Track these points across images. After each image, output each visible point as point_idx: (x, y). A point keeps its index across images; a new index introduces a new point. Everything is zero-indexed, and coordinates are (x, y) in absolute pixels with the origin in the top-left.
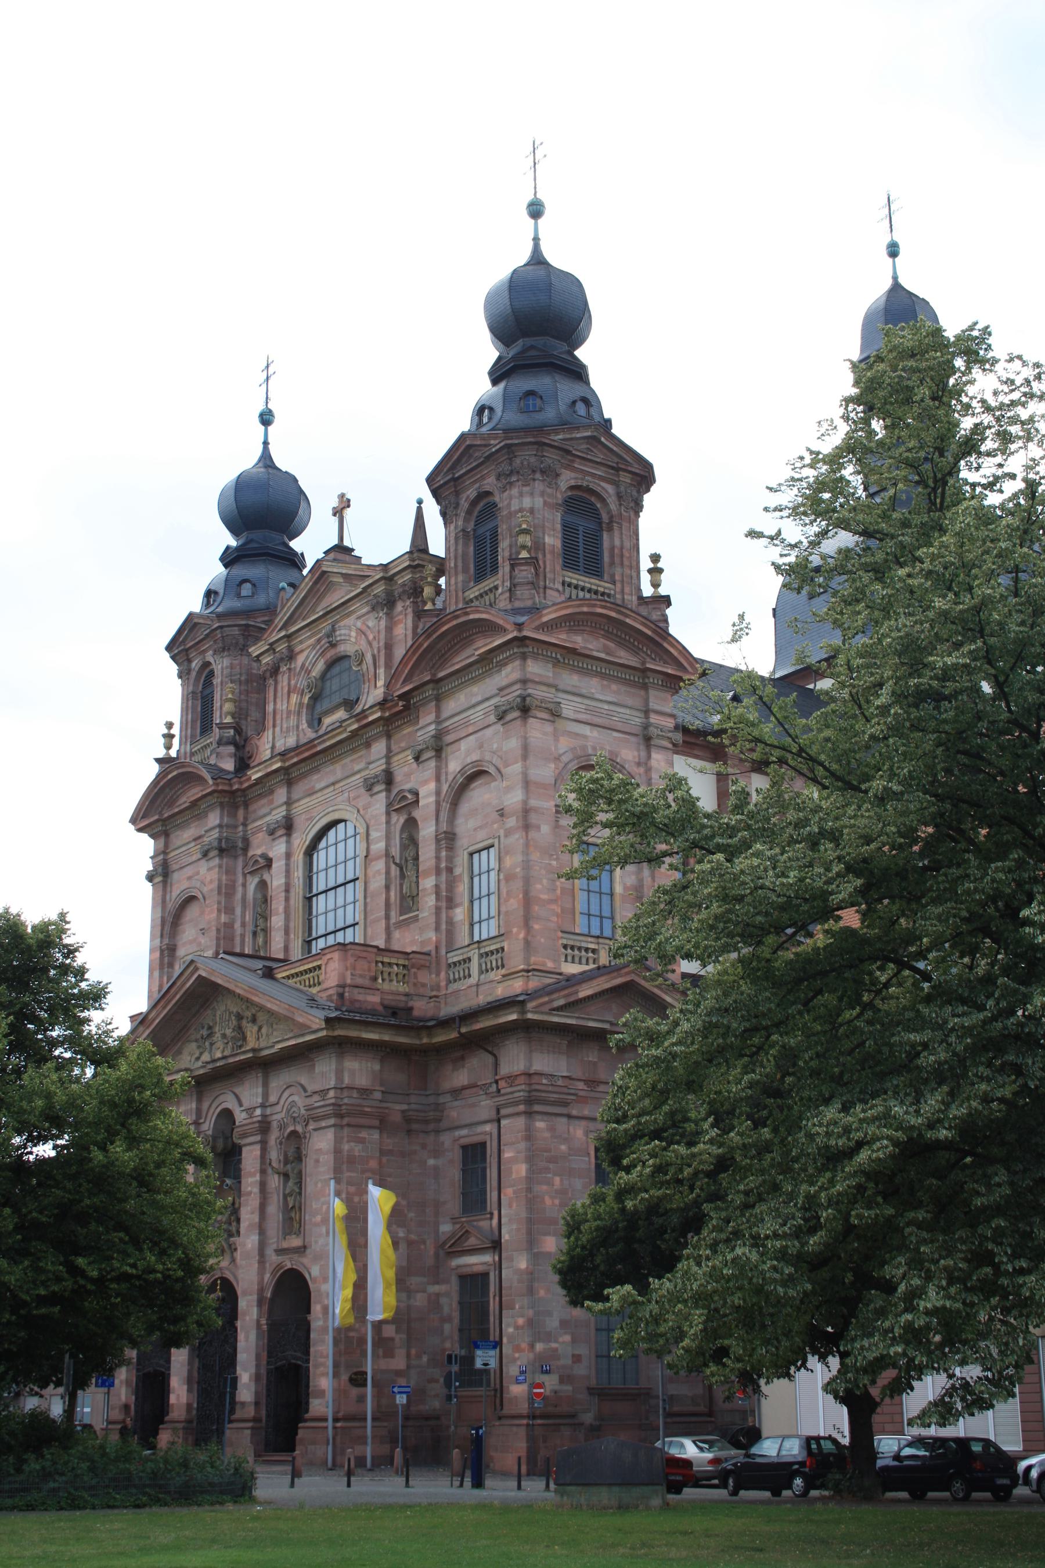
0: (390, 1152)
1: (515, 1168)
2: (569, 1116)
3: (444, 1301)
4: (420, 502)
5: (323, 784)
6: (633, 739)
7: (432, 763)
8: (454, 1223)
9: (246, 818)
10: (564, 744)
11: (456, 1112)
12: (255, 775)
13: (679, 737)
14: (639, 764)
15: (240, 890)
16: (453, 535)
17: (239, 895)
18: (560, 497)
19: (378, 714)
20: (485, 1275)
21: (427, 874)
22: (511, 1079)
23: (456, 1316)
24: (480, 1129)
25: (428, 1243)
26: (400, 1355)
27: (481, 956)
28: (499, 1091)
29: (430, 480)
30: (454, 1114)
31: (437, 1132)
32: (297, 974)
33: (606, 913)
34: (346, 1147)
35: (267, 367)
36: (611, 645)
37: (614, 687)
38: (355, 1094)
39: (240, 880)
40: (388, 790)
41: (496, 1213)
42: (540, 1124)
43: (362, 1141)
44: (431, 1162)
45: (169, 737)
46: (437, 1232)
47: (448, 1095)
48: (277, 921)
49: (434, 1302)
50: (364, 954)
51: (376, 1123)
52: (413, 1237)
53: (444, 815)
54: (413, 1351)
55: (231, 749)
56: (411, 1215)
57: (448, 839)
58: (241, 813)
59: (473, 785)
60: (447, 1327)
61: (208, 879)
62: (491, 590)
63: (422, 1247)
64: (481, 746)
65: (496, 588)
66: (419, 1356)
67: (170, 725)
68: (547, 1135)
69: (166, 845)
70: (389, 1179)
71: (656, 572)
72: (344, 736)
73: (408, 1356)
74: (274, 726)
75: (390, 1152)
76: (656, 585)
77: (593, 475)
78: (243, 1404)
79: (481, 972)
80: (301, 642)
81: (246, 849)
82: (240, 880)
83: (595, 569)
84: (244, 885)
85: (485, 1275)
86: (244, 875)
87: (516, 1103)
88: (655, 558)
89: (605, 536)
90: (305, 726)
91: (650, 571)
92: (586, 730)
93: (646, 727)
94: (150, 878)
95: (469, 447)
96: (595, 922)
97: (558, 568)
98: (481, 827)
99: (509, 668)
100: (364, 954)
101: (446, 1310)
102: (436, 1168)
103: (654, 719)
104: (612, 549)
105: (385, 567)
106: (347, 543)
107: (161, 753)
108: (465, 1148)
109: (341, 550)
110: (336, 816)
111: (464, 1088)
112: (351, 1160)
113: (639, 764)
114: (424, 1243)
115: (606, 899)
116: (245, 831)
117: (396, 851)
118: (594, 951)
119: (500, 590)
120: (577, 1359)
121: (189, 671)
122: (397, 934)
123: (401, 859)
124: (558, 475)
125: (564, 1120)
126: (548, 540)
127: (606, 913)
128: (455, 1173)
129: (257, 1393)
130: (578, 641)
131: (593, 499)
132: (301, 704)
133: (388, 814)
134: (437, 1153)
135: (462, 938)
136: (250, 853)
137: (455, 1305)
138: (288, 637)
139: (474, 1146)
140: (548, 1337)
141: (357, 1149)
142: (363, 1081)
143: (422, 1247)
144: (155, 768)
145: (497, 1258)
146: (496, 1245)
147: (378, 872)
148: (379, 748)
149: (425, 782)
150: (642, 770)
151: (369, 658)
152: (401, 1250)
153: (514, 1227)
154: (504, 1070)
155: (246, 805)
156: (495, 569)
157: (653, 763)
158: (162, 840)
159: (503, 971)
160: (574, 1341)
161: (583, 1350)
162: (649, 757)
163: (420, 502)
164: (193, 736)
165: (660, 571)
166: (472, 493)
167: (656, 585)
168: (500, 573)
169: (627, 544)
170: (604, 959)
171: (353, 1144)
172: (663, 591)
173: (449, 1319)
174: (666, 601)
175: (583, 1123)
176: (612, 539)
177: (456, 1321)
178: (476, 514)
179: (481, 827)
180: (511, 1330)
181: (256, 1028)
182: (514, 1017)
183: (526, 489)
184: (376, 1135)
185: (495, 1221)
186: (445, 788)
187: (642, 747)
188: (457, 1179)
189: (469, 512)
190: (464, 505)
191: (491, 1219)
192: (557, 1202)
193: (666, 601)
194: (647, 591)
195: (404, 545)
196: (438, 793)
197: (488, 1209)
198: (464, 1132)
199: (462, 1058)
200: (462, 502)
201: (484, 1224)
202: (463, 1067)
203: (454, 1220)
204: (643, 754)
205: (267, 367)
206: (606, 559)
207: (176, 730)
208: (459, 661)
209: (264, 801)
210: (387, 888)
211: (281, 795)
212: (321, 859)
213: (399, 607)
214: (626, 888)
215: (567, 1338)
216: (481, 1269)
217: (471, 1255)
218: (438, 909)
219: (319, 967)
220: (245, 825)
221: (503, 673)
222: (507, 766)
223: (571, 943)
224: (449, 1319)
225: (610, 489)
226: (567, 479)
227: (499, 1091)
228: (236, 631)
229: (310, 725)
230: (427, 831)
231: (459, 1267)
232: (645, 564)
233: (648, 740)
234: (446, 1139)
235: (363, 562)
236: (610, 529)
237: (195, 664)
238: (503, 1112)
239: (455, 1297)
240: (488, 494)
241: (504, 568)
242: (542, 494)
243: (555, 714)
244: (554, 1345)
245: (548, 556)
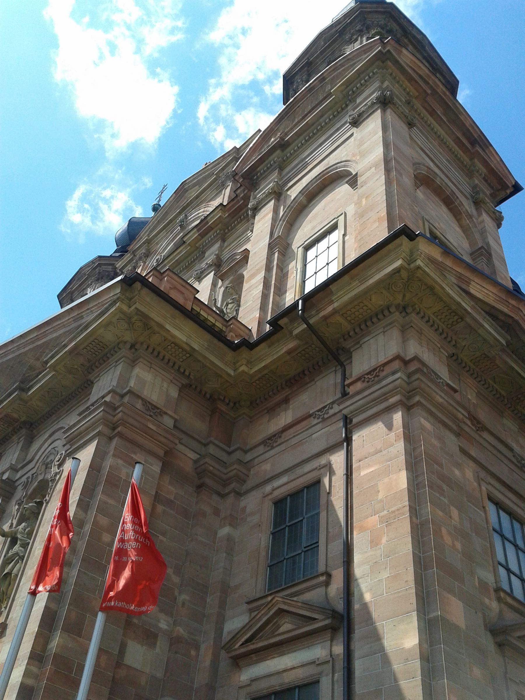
8: (251, 611)
24: (308, 467)
25: (203, 647)
31: (239, 494)
38: (139, 405)
44: (225, 531)
46: (219, 630)
47: (262, 447)
50: (182, 289)
51: (161, 453)
52: (180, 630)
56: (184, 597)
63: (193, 653)
70: (161, 537)
75: (169, 503)
80: (157, 244)
87: (385, 397)
100: (182, 289)
102: (229, 539)
108: (279, 504)
114: (197, 648)
123: (222, 305)
139: (296, 495)
143: (193, 653)
145: (339, 649)
152: (158, 650)
153: (385, 575)
171: (120, 462)
188: (263, 544)
191: (327, 584)
197: (322, 568)
199: (286, 401)
202: (286, 410)
216: (300, 675)
217: (282, 654)
231: (253, 680)
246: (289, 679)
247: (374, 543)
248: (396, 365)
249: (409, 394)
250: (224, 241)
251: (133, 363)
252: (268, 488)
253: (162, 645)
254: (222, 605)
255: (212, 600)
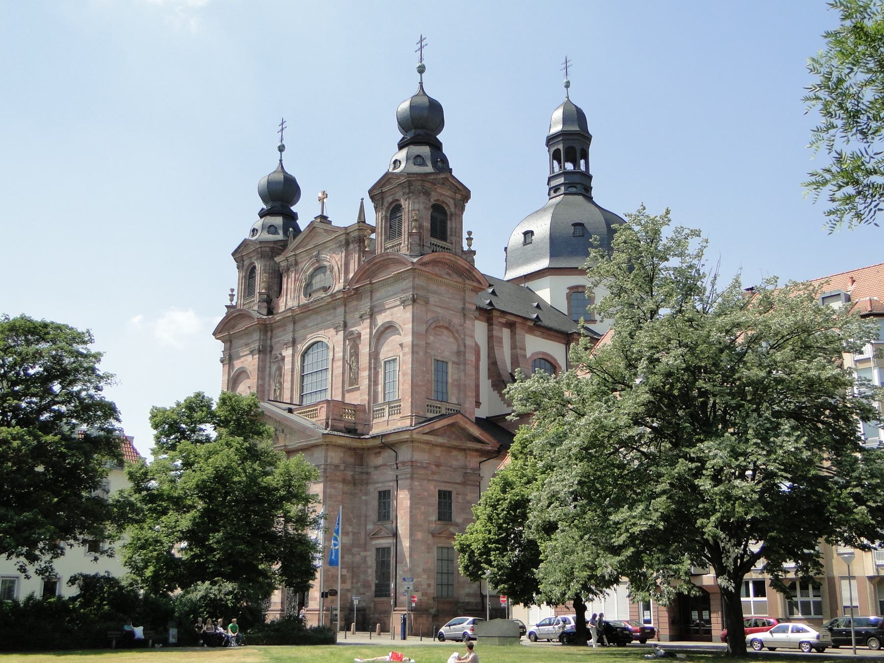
0: (346, 493)
1: (405, 502)
2: (428, 480)
3: (367, 559)
4: (362, 199)
5: (311, 325)
6: (458, 314)
7: (369, 320)
9: (271, 337)
10: (430, 316)
11: (375, 475)
12: (278, 318)
13: (477, 314)
14: (460, 325)
15: (268, 369)
16: (380, 218)
17: (267, 372)
18: (431, 204)
19: (342, 296)
20: (389, 548)
21: (364, 370)
22: (404, 463)
23: (374, 565)
24: (388, 484)
26: (349, 582)
27: (389, 408)
28: (397, 468)
29: (370, 192)
30: (375, 477)
32: (304, 412)
33: (440, 390)
34: (328, 490)
35: (282, 124)
36: (450, 271)
37: (451, 291)
39: (268, 365)
40: (344, 330)
41: (395, 521)
42: (416, 483)
43: (334, 488)
44: (364, 498)
45: (232, 296)
46: (366, 529)
48: (287, 385)
49: (365, 559)
52: (355, 530)
53: (373, 345)
54: (354, 581)
55: (265, 304)
57: (374, 355)
58: (269, 334)
59: (387, 332)
60: (370, 571)
61: (253, 363)
62: (398, 245)
64: (392, 315)
65: (401, 244)
66: (357, 583)
67: (232, 290)
68: (419, 488)
69: (230, 347)
71: (470, 239)
72: (324, 304)
73: (352, 583)
74: (287, 295)
76: (470, 245)
77: (444, 195)
78: (275, 603)
79: (389, 415)
80: (301, 258)
81: (271, 351)
82: (268, 365)
83: (444, 238)
84: (270, 367)
85: (389, 548)
86: (270, 362)
88: (470, 233)
89: (449, 222)
90: (303, 296)
91: (467, 239)
92: (439, 310)
93: (463, 309)
94: (222, 361)
95: (389, 179)
96: (440, 395)
97: (429, 236)
98: (391, 351)
99: (407, 281)
101: (369, 563)
102: (366, 500)
103: (467, 305)
104: (451, 228)
105: (346, 228)
106: (325, 214)
107: (229, 303)
108: (380, 492)
109: (323, 218)
110: (318, 339)
111: (380, 466)
112: (331, 497)
113: (460, 325)
115: (444, 385)
116: (271, 343)
117: (348, 357)
118: (439, 408)
119: (402, 245)
120: (429, 585)
121: (243, 266)
122: (347, 395)
124: (430, 195)
125: (426, 482)
126: (425, 224)
127: (444, 391)
128: (374, 503)
129: (282, 599)
130: (436, 270)
131: (444, 206)
132: (301, 287)
133: (344, 341)
134: (366, 494)
135: (381, 400)
136: (273, 353)
137: (374, 561)
138: (295, 255)
139: (384, 492)
140: (418, 576)
141: (333, 492)
142: (336, 461)
144: (226, 310)
146: (395, 535)
147: (339, 366)
148: (341, 310)
149: (365, 328)
150: (461, 328)
151: (336, 269)
154: (400, 459)
155: (272, 331)
156: (400, 234)
157: (466, 325)
158: (228, 344)
159: (401, 415)
160: (428, 578)
161: (432, 582)
162: (465, 323)
163: (362, 199)
164: (244, 297)
165: (472, 239)
166: (390, 199)
167: (470, 245)
168: (403, 237)
169: (458, 227)
170: (444, 412)
172: (472, 248)
173: (371, 567)
174: (474, 253)
175: (434, 483)
176: (451, 224)
177: (374, 568)
178: (391, 209)
179: (391, 351)
180: (401, 572)
181: (284, 436)
182: (408, 436)
183: (416, 200)
184: (340, 486)
185: (394, 525)
186: (374, 331)
187: (462, 318)
189: (388, 208)
190: (386, 204)
192: (422, 517)
193: (474, 253)
194: (466, 248)
195: (355, 220)
196: (371, 333)
198: (380, 485)
199: (380, 452)
200: (385, 203)
201: (389, 526)
203: (374, 524)
204: (462, 321)
205: (282, 124)
206: (449, 233)
207: (235, 293)
208: (382, 276)
209: (281, 329)
210: (343, 374)
211: (290, 327)
212: (309, 359)
213: (351, 246)
214: (453, 380)
215: (425, 576)
216: (387, 546)
218: (370, 386)
219: (316, 410)
220: (271, 340)
221: (404, 283)
222: (405, 325)
223: (430, 404)
224: (371, 567)
225: (452, 201)
226: (434, 197)
227: (397, 468)
228: (268, 249)
229: (305, 295)
230: (364, 350)
232: (465, 236)
233: (465, 315)
234: (371, 488)
235: (333, 224)
236: (451, 220)
237: (246, 263)
238: (399, 477)
239: (374, 557)
240: (398, 200)
241: (405, 236)
242: (423, 203)
243: (427, 302)
244: (420, 579)
245: (425, 232)
246: (384, 546)
247: (402, 518)
248: (410, 463)
249: (412, 474)
250: (345, 306)
251: (327, 450)
252: (377, 485)
253: (351, 535)
254: (366, 521)
255: (363, 519)
